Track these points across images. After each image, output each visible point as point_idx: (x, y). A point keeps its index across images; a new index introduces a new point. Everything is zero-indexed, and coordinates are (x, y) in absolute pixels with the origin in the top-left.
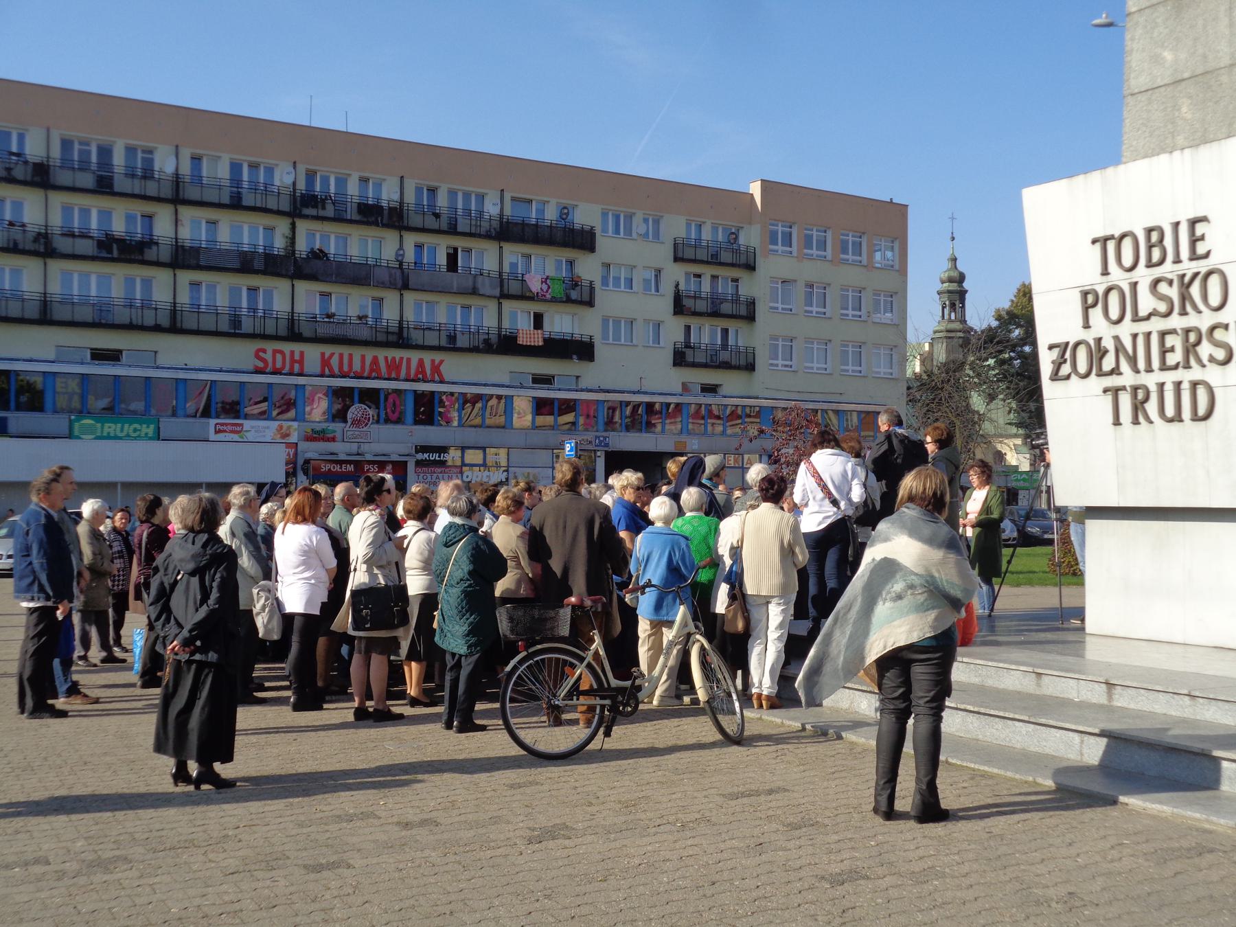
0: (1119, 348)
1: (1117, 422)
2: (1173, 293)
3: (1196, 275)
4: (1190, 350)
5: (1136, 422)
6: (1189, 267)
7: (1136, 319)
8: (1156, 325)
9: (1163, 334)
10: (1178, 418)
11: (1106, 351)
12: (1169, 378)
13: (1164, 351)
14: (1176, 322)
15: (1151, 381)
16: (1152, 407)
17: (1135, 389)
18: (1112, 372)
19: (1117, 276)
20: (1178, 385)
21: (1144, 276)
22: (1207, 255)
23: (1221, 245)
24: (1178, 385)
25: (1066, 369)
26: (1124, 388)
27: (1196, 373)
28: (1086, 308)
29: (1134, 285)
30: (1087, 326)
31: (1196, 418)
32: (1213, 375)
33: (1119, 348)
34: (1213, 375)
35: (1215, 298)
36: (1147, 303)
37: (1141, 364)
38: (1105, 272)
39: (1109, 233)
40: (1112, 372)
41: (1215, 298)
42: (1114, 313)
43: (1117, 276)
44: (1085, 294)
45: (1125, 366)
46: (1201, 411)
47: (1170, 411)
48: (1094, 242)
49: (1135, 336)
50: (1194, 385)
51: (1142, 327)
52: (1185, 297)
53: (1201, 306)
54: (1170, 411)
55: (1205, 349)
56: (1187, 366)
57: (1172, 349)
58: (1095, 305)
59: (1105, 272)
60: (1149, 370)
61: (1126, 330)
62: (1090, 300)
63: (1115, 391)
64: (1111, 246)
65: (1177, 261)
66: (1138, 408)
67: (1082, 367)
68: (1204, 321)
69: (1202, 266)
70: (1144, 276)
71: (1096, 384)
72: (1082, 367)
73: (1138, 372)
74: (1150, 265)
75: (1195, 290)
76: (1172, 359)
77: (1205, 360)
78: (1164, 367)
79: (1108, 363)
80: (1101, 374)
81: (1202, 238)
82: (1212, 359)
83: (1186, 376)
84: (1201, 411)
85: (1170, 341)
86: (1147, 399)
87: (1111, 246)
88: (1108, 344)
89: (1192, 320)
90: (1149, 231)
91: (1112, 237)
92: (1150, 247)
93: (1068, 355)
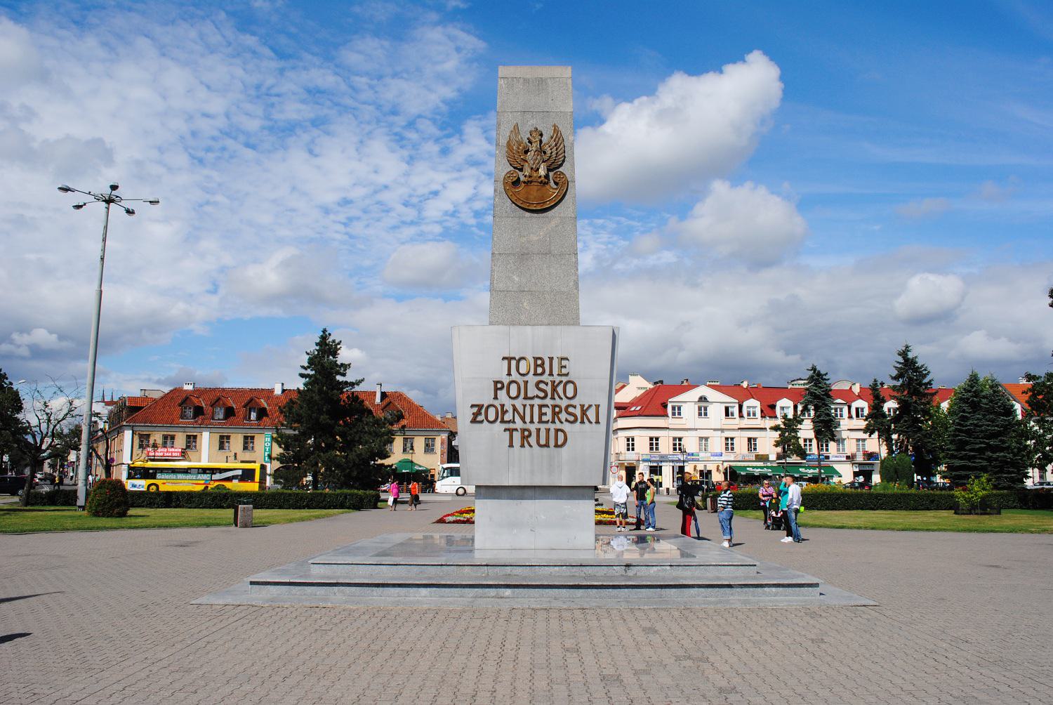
0: (515, 409)
1: (511, 445)
2: (549, 389)
3: (561, 382)
4: (555, 414)
5: (522, 446)
6: (558, 379)
7: (526, 398)
8: (537, 402)
9: (541, 407)
10: (547, 445)
11: (507, 411)
12: (543, 427)
13: (541, 414)
14: (548, 401)
15: (533, 428)
16: (533, 440)
17: (523, 430)
18: (509, 422)
19: (515, 376)
20: (548, 430)
21: (532, 379)
22: (567, 375)
23: (574, 370)
24: (548, 430)
25: (479, 418)
26: (516, 430)
27: (558, 425)
28: (496, 389)
29: (526, 383)
30: (496, 398)
31: (556, 446)
32: (566, 427)
33: (515, 409)
34: (566, 427)
35: (570, 394)
36: (532, 391)
37: (528, 419)
38: (509, 374)
39: (512, 356)
40: (509, 422)
41: (570, 393)
42: (513, 393)
43: (515, 376)
44: (496, 383)
45: (517, 419)
46: (560, 443)
47: (543, 442)
48: (504, 358)
49: (525, 406)
50: (557, 431)
51: (528, 402)
52: (554, 389)
53: (562, 396)
54: (543, 442)
55: (563, 416)
56: (553, 422)
57: (545, 414)
58: (501, 388)
59: (509, 374)
60: (532, 422)
61: (519, 403)
62: (498, 386)
63: (511, 431)
64: (513, 363)
65: (551, 374)
66: (525, 437)
67: (492, 417)
68: (564, 403)
69: (565, 379)
70: (532, 379)
71: (499, 427)
72: (492, 417)
73: (525, 422)
74: (535, 374)
75: (560, 389)
76: (544, 418)
77: (563, 420)
78: (540, 421)
79: (508, 417)
80: (503, 421)
81: (565, 367)
82: (567, 420)
83: (552, 427)
84: (560, 443)
85: (544, 410)
86: (530, 435)
87: (513, 363)
88: (508, 407)
89: (558, 401)
90: (536, 359)
91: (514, 358)
92: (536, 366)
93: (483, 411)
